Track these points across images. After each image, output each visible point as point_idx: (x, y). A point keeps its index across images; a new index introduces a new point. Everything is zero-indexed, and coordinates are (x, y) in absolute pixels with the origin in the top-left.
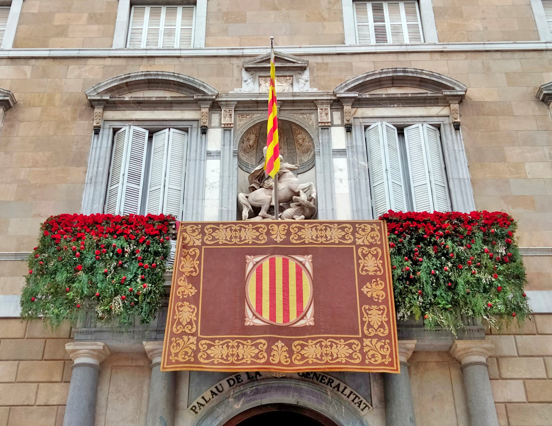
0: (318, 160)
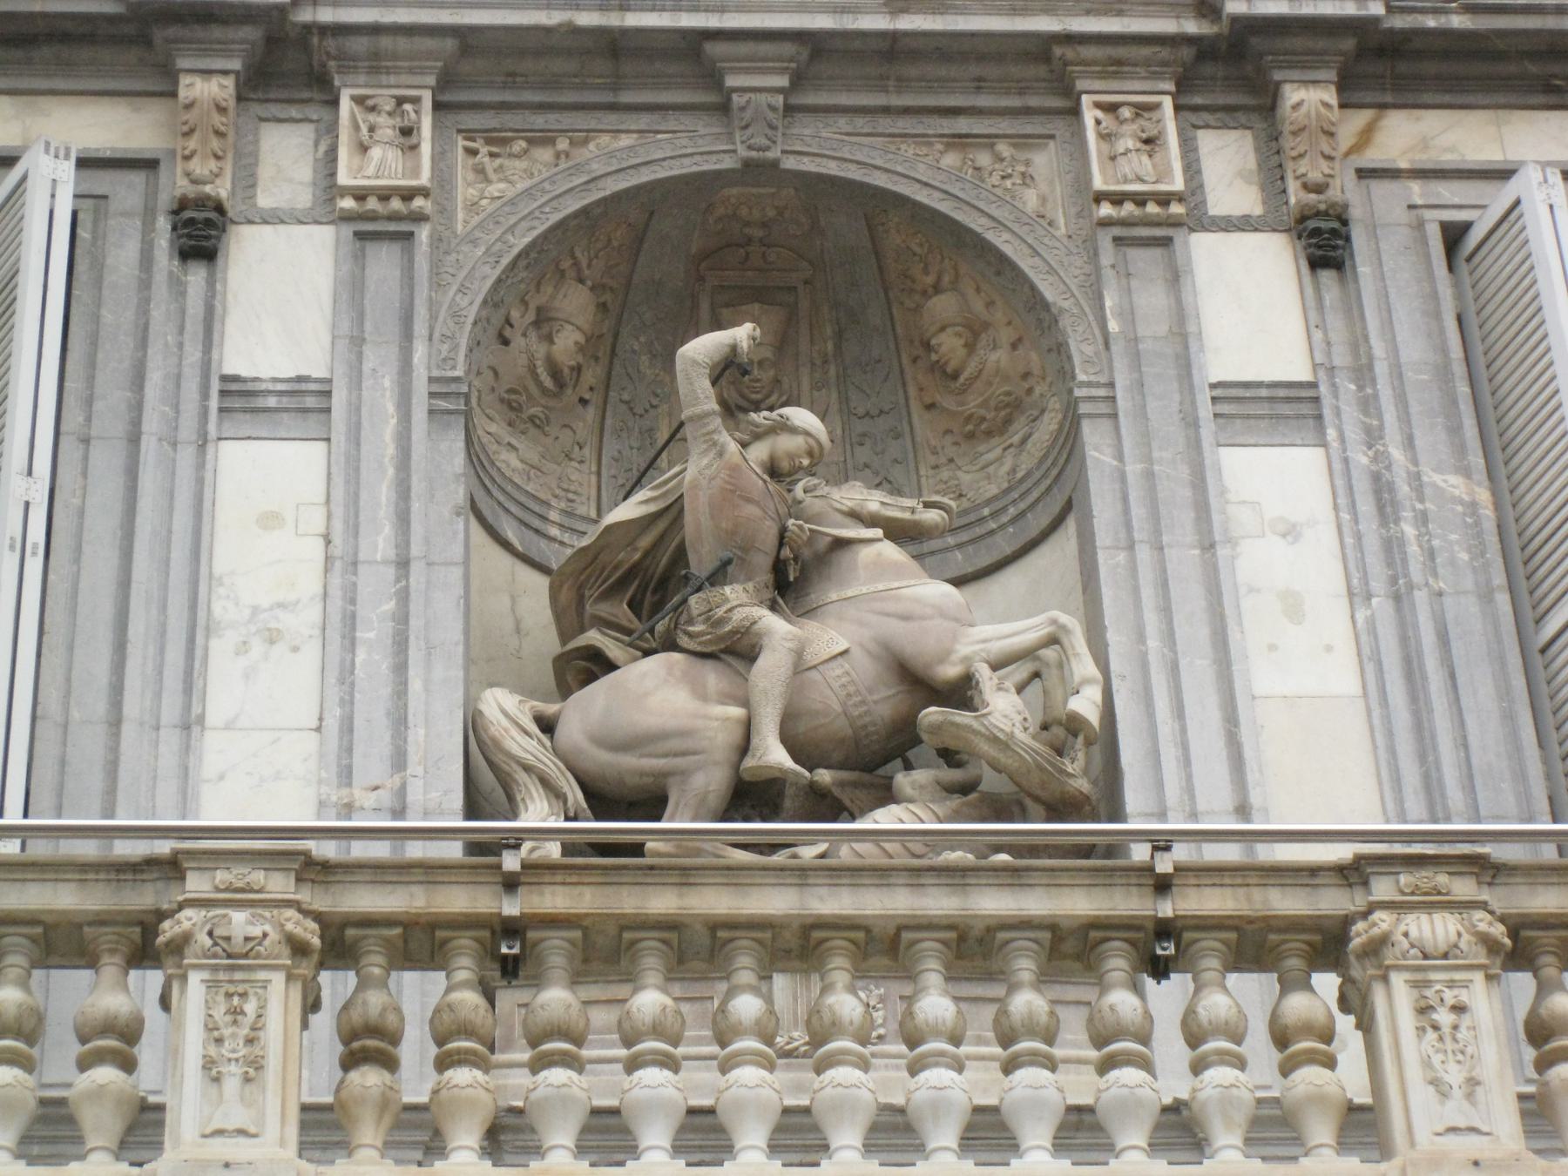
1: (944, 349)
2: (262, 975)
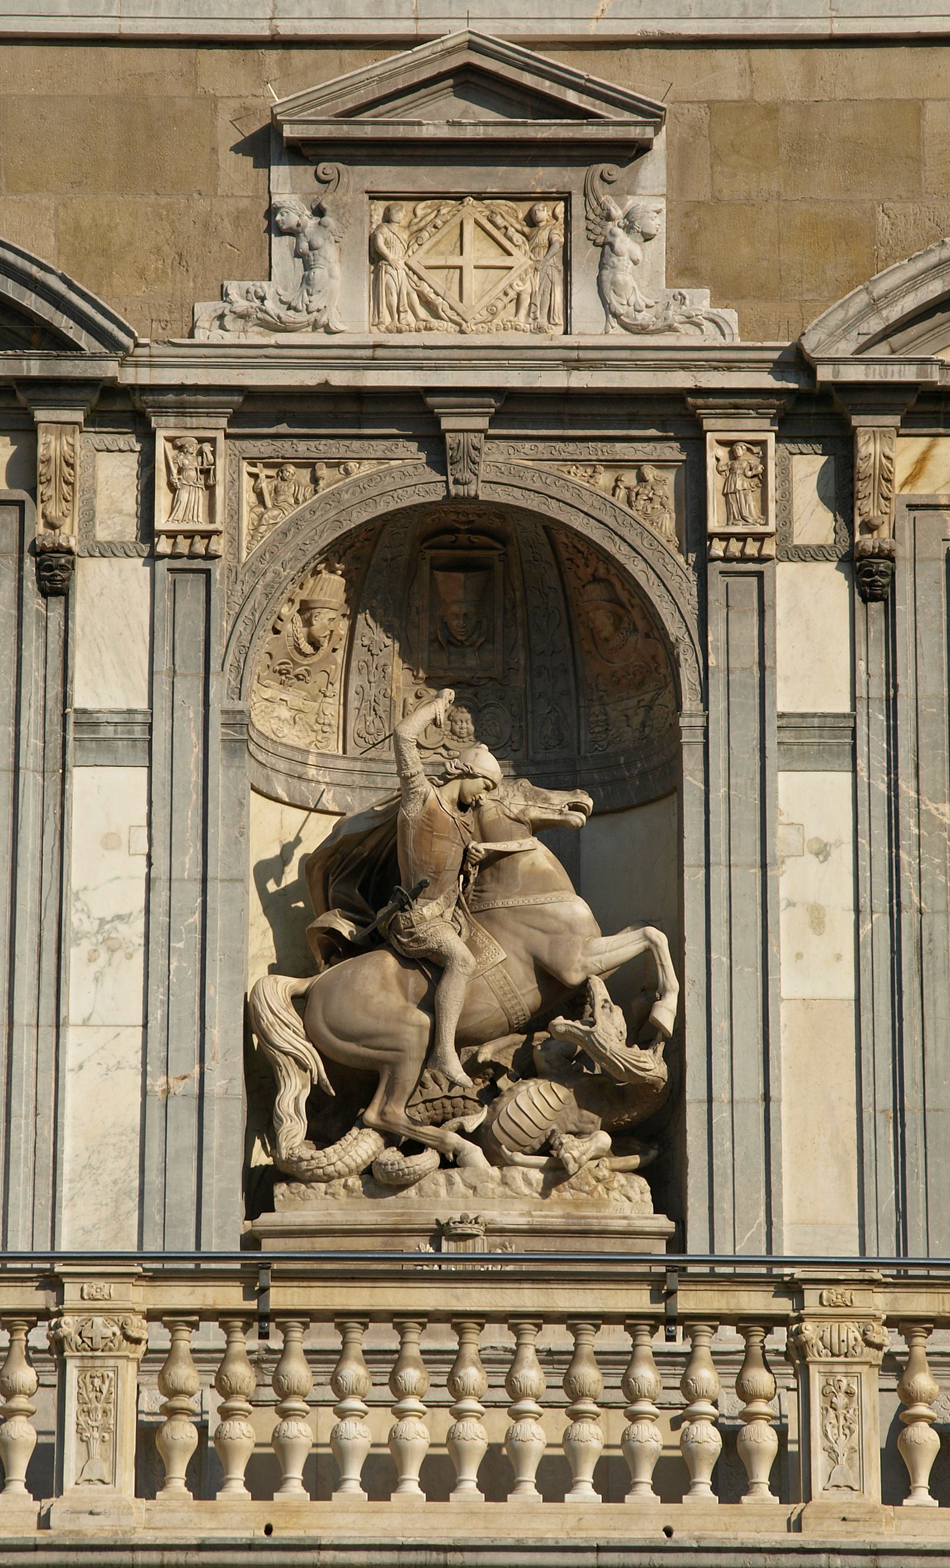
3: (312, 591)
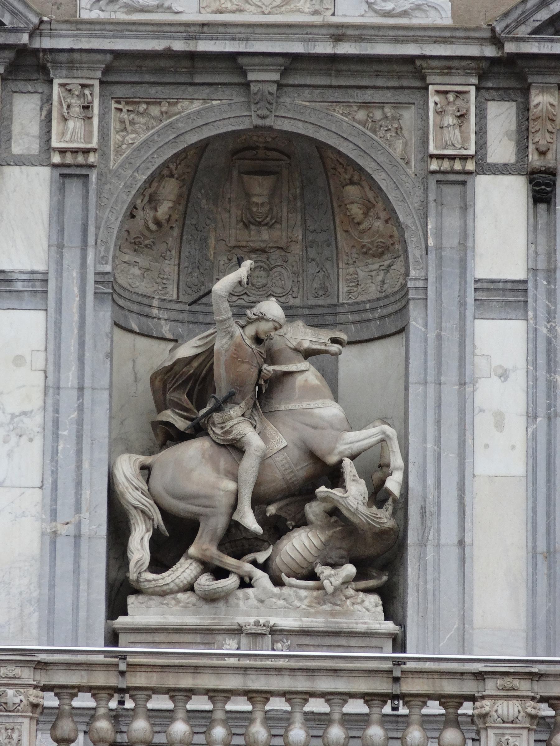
0: (415, 323)
1: (352, 212)
2: (20, 720)
3: (158, 188)
